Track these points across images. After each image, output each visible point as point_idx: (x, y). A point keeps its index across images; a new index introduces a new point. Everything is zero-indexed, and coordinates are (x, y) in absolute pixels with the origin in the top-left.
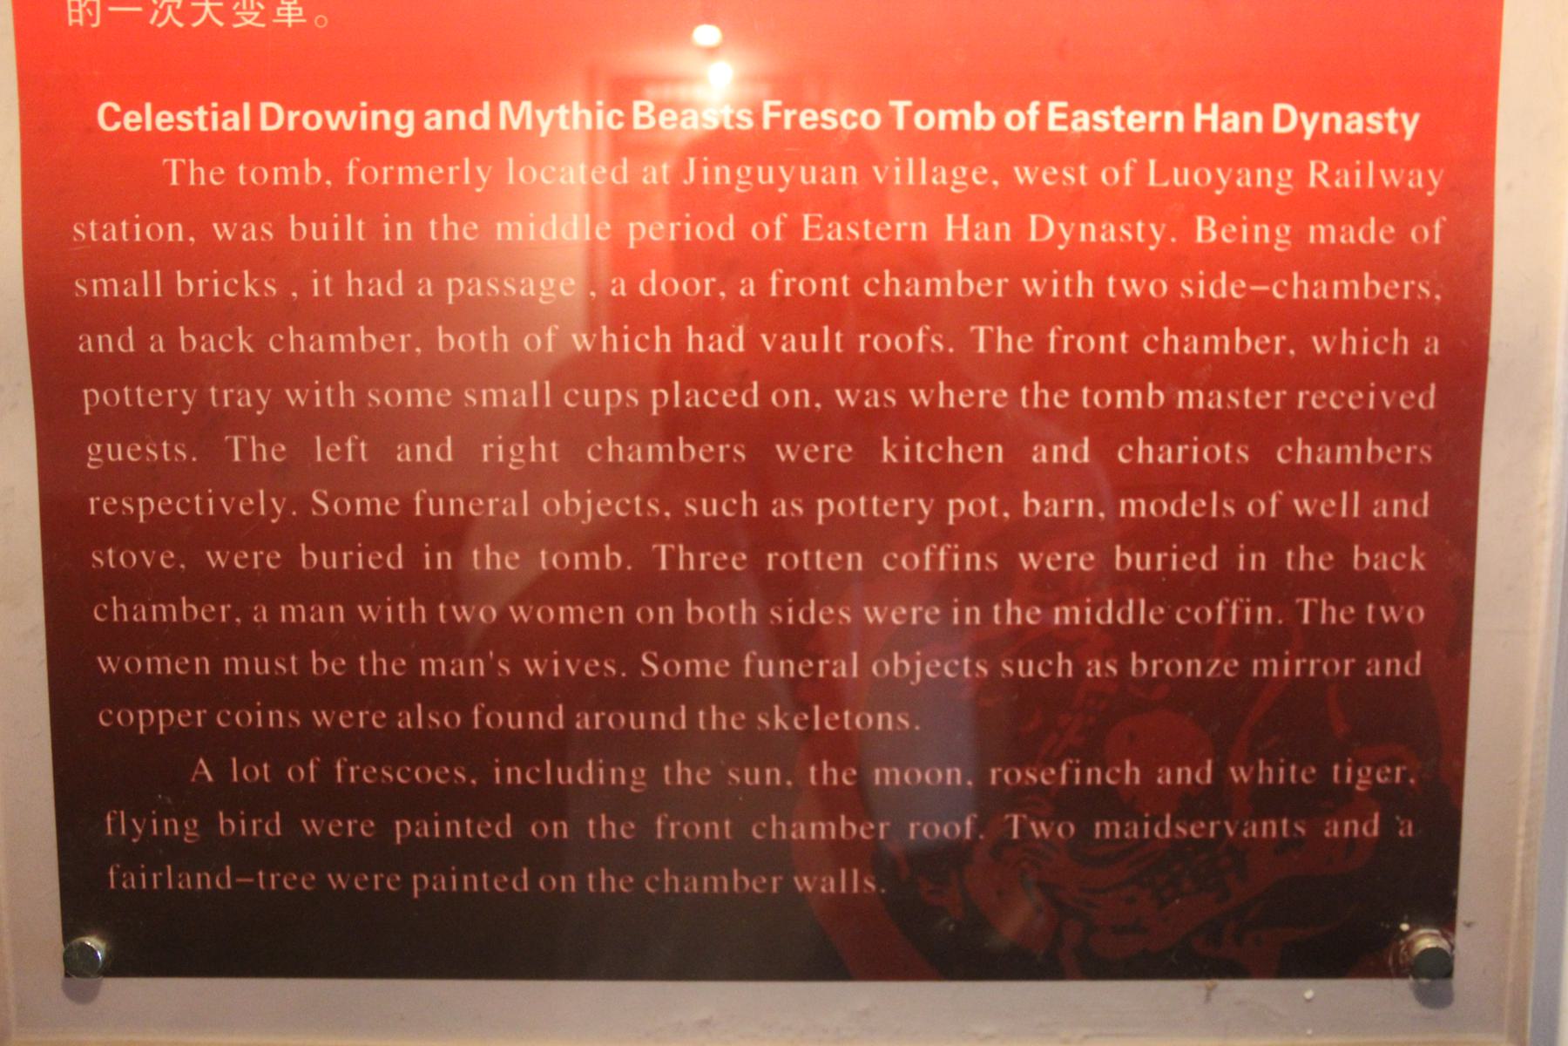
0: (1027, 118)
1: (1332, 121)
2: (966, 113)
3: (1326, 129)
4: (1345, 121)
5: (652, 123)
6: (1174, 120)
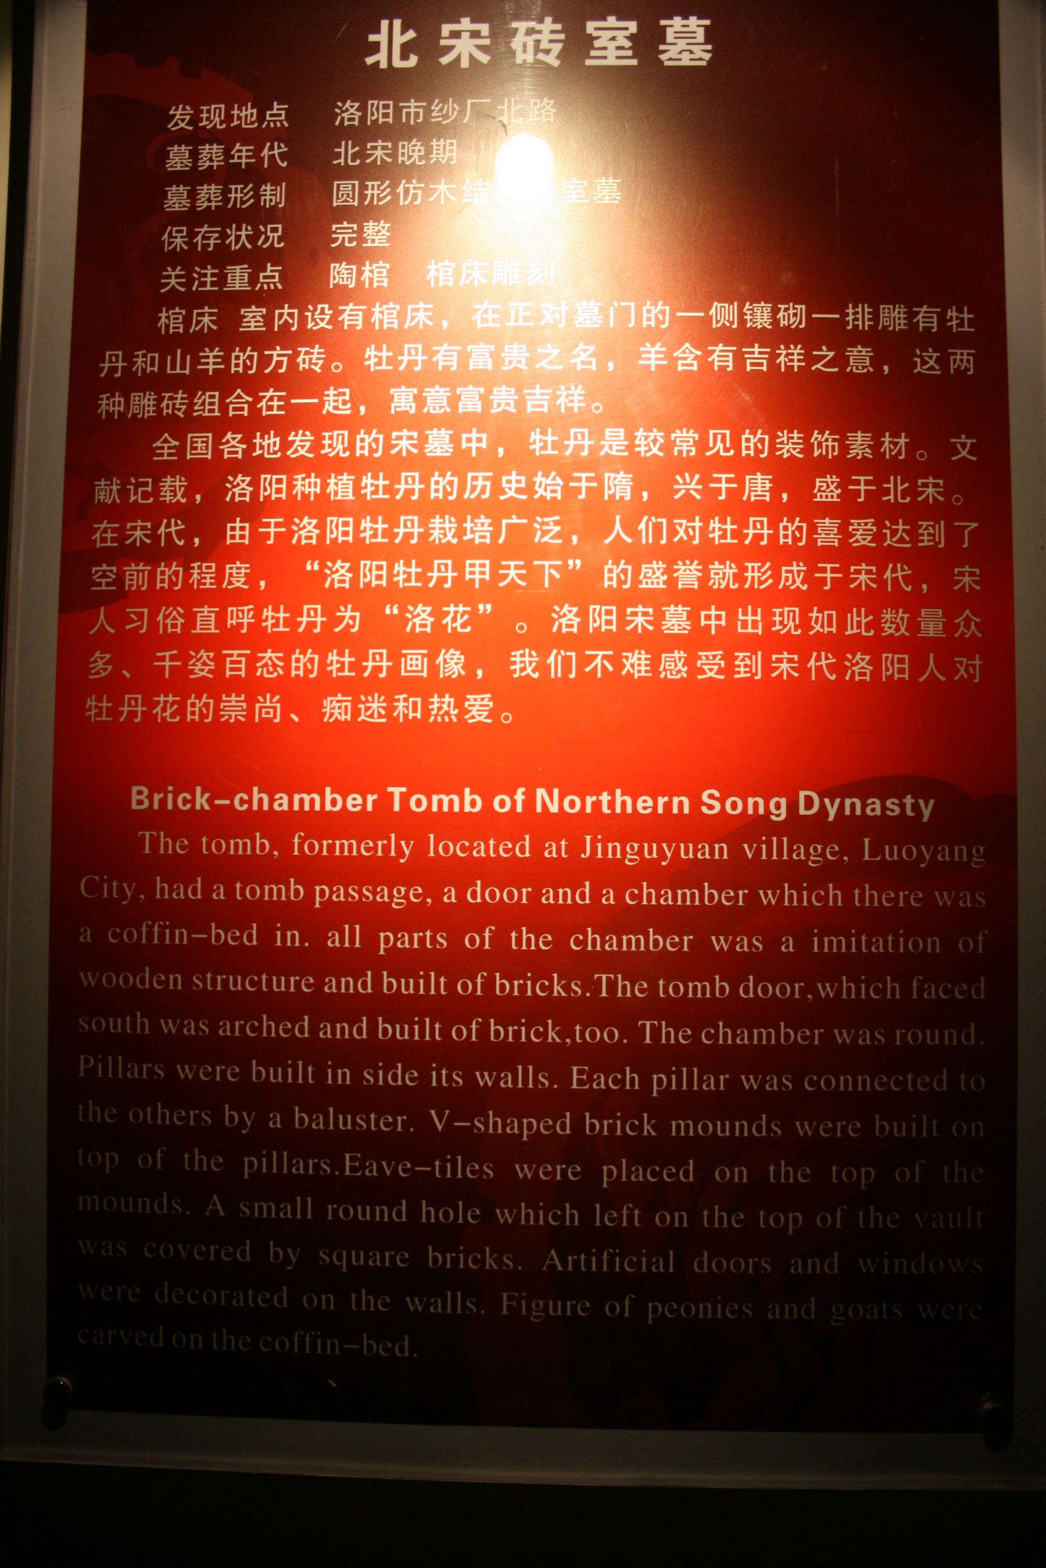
0: (514, 803)
1: (853, 805)
2: (456, 799)
3: (847, 812)
4: (864, 806)
5: (146, 804)
6: (681, 804)
